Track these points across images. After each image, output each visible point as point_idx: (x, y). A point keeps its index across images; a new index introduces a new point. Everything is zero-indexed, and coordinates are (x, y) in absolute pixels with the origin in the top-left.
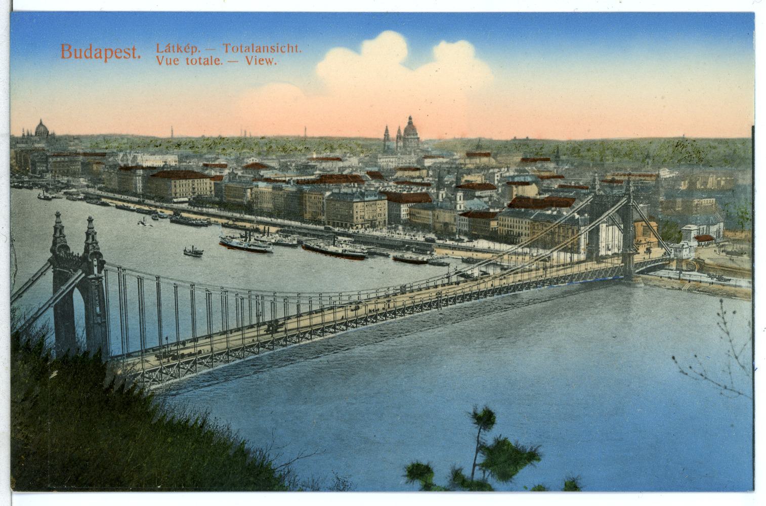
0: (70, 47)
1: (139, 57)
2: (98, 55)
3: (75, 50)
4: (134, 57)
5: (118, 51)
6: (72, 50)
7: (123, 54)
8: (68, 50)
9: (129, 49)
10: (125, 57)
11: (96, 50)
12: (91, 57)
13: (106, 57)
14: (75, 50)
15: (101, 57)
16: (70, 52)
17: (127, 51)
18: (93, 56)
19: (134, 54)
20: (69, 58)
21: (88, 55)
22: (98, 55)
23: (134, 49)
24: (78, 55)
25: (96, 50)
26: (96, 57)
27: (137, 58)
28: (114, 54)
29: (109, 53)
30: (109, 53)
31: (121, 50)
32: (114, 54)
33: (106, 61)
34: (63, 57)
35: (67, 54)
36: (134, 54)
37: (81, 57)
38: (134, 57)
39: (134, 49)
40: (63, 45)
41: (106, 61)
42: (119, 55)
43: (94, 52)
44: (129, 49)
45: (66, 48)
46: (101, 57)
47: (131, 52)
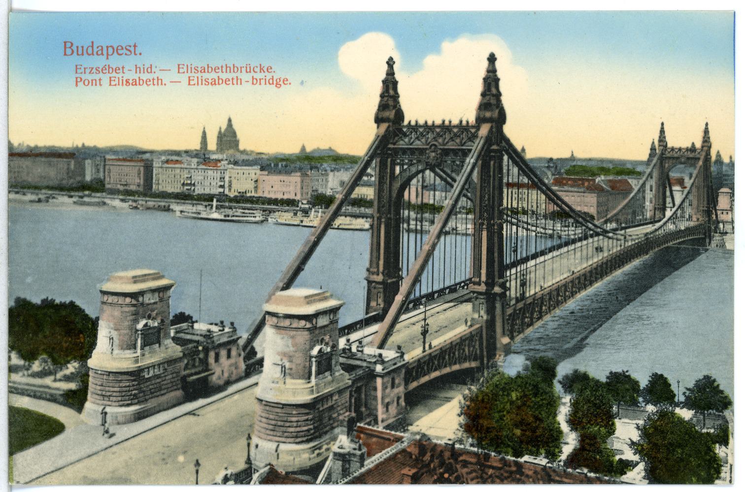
0: (72, 44)
1: (140, 54)
2: (100, 52)
3: (77, 47)
4: (135, 54)
5: (120, 48)
6: (74, 48)
7: (125, 51)
8: (70, 48)
9: (130, 46)
10: (126, 54)
11: (98, 47)
12: (93, 54)
13: (108, 55)
14: (77, 47)
15: (102, 54)
16: (72, 50)
17: (128, 48)
18: (95, 53)
19: (135, 52)
20: (72, 54)
21: (90, 51)
22: (100, 52)
23: (135, 46)
24: (80, 52)
25: (98, 47)
26: (97, 54)
27: (138, 55)
28: (115, 51)
29: (110, 50)
30: (110, 50)
31: (122, 47)
32: (115, 51)
33: (107, 58)
34: (65, 54)
35: (69, 51)
36: (135, 52)
37: (83, 54)
38: (135, 54)
39: (135, 46)
40: (65, 43)
41: (107, 58)
42: (120, 52)
43: (95, 50)
44: (130, 46)
45: (68, 45)
46: (102, 54)
47: (132, 49)
